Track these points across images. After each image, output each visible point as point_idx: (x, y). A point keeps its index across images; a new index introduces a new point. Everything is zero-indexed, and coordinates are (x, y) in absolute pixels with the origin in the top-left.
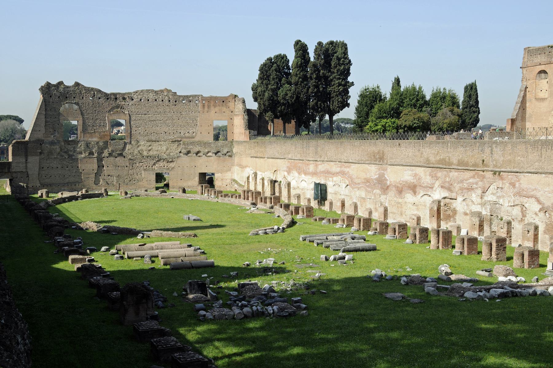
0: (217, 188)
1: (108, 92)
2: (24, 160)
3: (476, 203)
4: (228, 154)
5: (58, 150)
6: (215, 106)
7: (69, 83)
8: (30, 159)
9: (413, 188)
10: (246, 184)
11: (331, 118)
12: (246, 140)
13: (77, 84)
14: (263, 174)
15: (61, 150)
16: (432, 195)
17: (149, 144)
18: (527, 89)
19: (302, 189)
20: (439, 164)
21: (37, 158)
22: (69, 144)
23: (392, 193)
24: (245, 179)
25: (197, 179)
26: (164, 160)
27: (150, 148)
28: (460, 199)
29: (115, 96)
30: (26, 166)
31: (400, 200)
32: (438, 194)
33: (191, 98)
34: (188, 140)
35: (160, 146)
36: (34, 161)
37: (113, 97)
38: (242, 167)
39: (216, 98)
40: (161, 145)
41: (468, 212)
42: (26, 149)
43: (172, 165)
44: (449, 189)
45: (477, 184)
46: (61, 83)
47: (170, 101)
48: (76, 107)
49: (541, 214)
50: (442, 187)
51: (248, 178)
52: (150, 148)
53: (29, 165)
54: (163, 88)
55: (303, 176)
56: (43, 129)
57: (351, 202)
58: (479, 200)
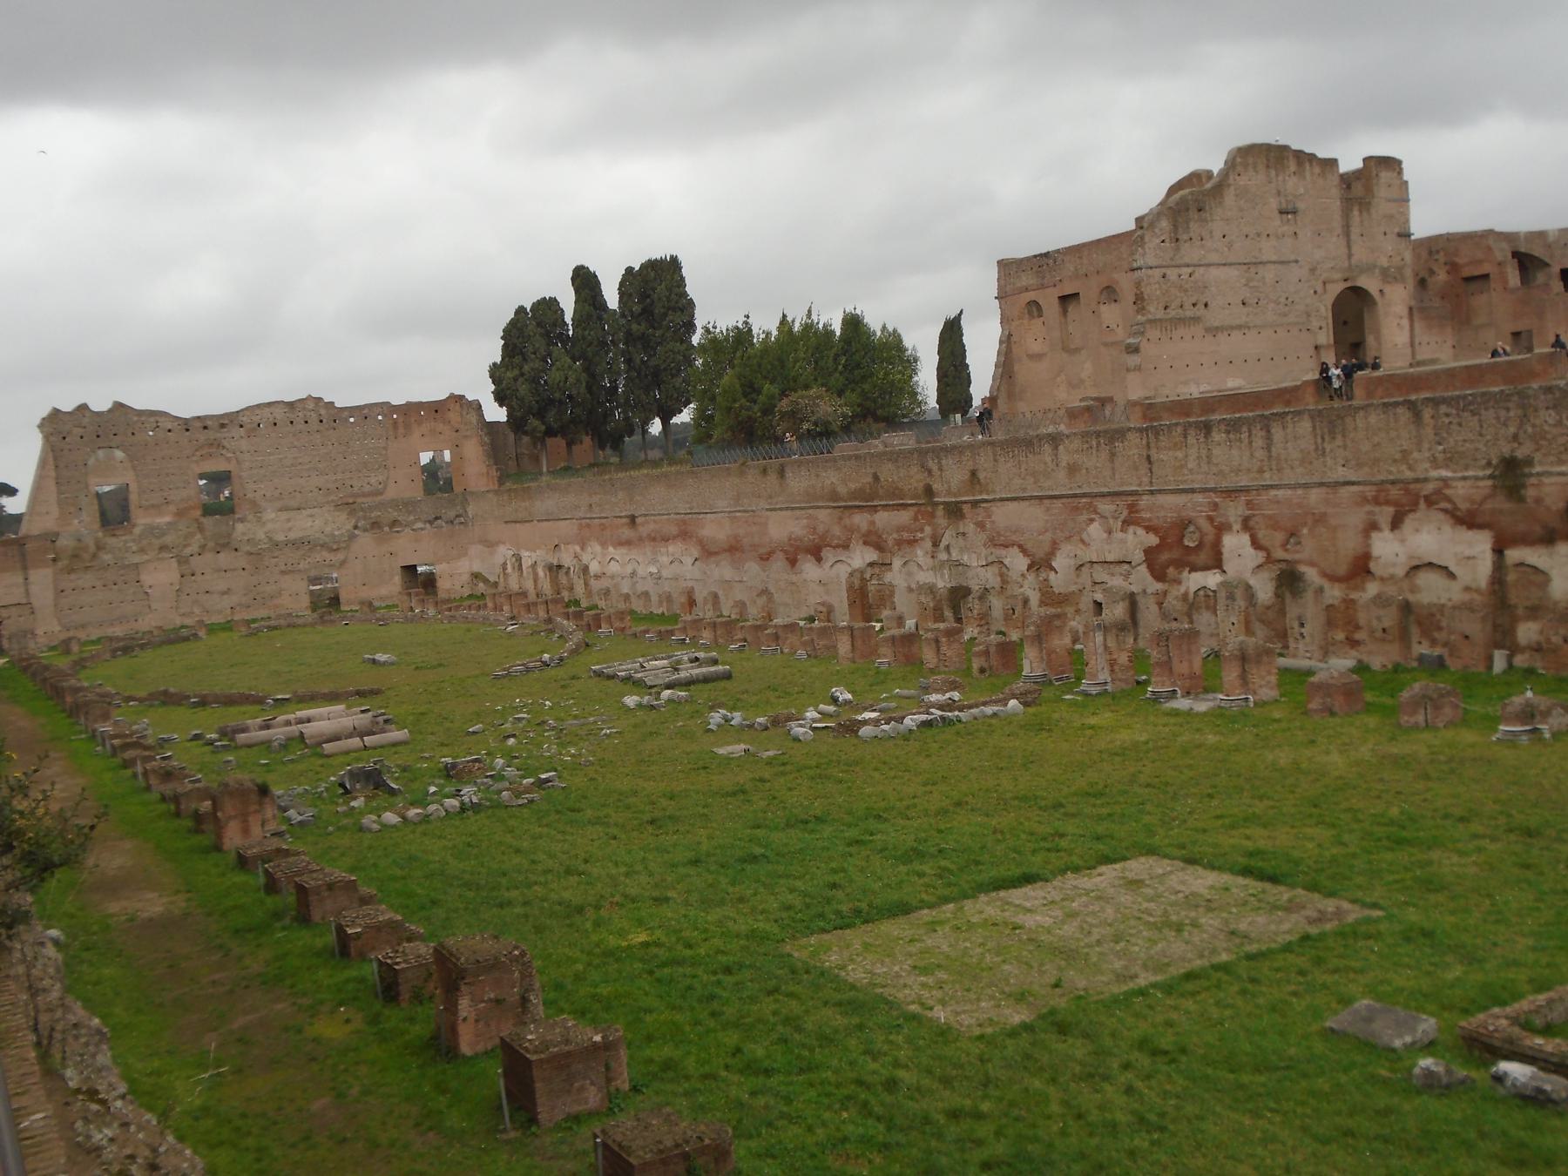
0: (442, 595)
1: (186, 415)
2: (20, 579)
3: (925, 568)
4: (457, 521)
5: (92, 548)
6: (419, 423)
7: (100, 404)
9: (816, 553)
10: (502, 580)
11: (665, 422)
12: (491, 487)
13: (119, 406)
14: (533, 554)
16: (849, 561)
17: (284, 515)
18: (1013, 339)
19: (612, 577)
20: (855, 499)
22: (114, 535)
23: (779, 563)
24: (499, 570)
25: (397, 579)
26: (322, 546)
27: (290, 524)
28: (897, 563)
29: (203, 423)
30: (27, 593)
31: (794, 578)
32: (861, 557)
33: (366, 411)
34: (369, 500)
35: (310, 519)
37: (199, 424)
38: (491, 545)
39: (420, 405)
40: (312, 516)
41: (914, 586)
42: (23, 556)
43: (341, 556)
44: (879, 547)
45: (922, 530)
46: (83, 408)
47: (321, 421)
48: (119, 454)
49: (1031, 577)
50: (865, 543)
51: (504, 566)
52: (290, 524)
53: (34, 589)
55: (611, 549)
56: (55, 511)
57: (705, 593)
58: (930, 561)
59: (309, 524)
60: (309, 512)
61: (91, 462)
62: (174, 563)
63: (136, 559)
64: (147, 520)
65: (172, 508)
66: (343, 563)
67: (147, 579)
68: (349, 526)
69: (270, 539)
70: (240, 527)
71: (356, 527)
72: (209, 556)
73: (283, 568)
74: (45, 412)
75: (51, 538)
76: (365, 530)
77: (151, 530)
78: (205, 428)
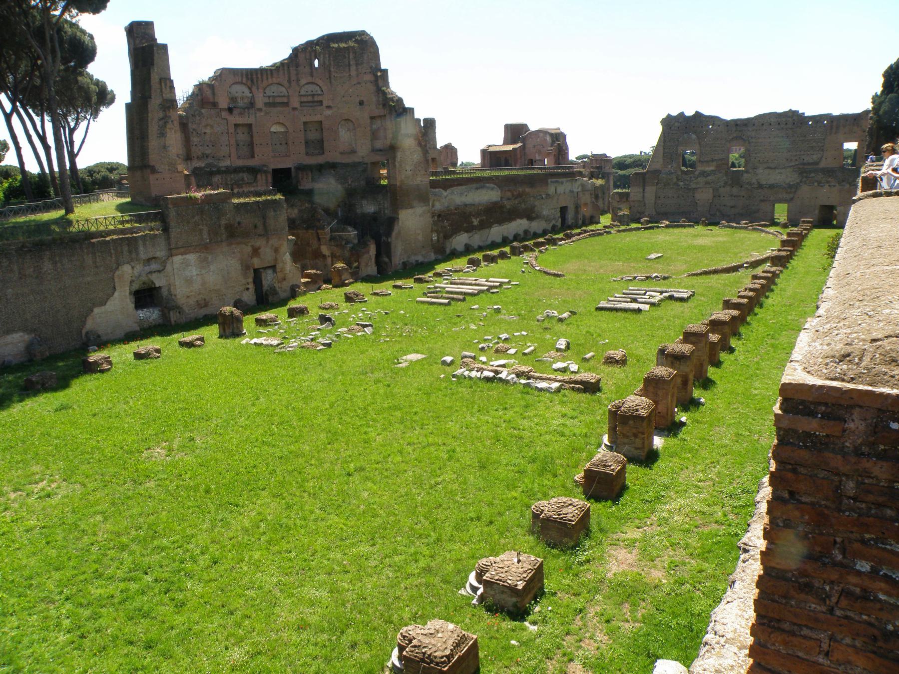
5: (675, 180)
7: (689, 113)
8: (648, 189)
15: (678, 180)
21: (654, 188)
30: (643, 197)
33: (818, 118)
34: (809, 167)
36: (651, 191)
46: (682, 114)
48: (694, 136)
53: (646, 194)
54: (787, 110)
56: (661, 160)
59: (779, 177)
60: (777, 171)
61: (681, 139)
62: (711, 190)
63: (694, 186)
64: (702, 169)
65: (714, 163)
66: (792, 199)
67: (698, 196)
68: (798, 181)
69: (759, 183)
70: (745, 175)
71: (801, 182)
72: (728, 188)
73: (762, 198)
74: (664, 116)
75: (656, 172)
76: (806, 183)
77: (704, 174)
78: (737, 125)
